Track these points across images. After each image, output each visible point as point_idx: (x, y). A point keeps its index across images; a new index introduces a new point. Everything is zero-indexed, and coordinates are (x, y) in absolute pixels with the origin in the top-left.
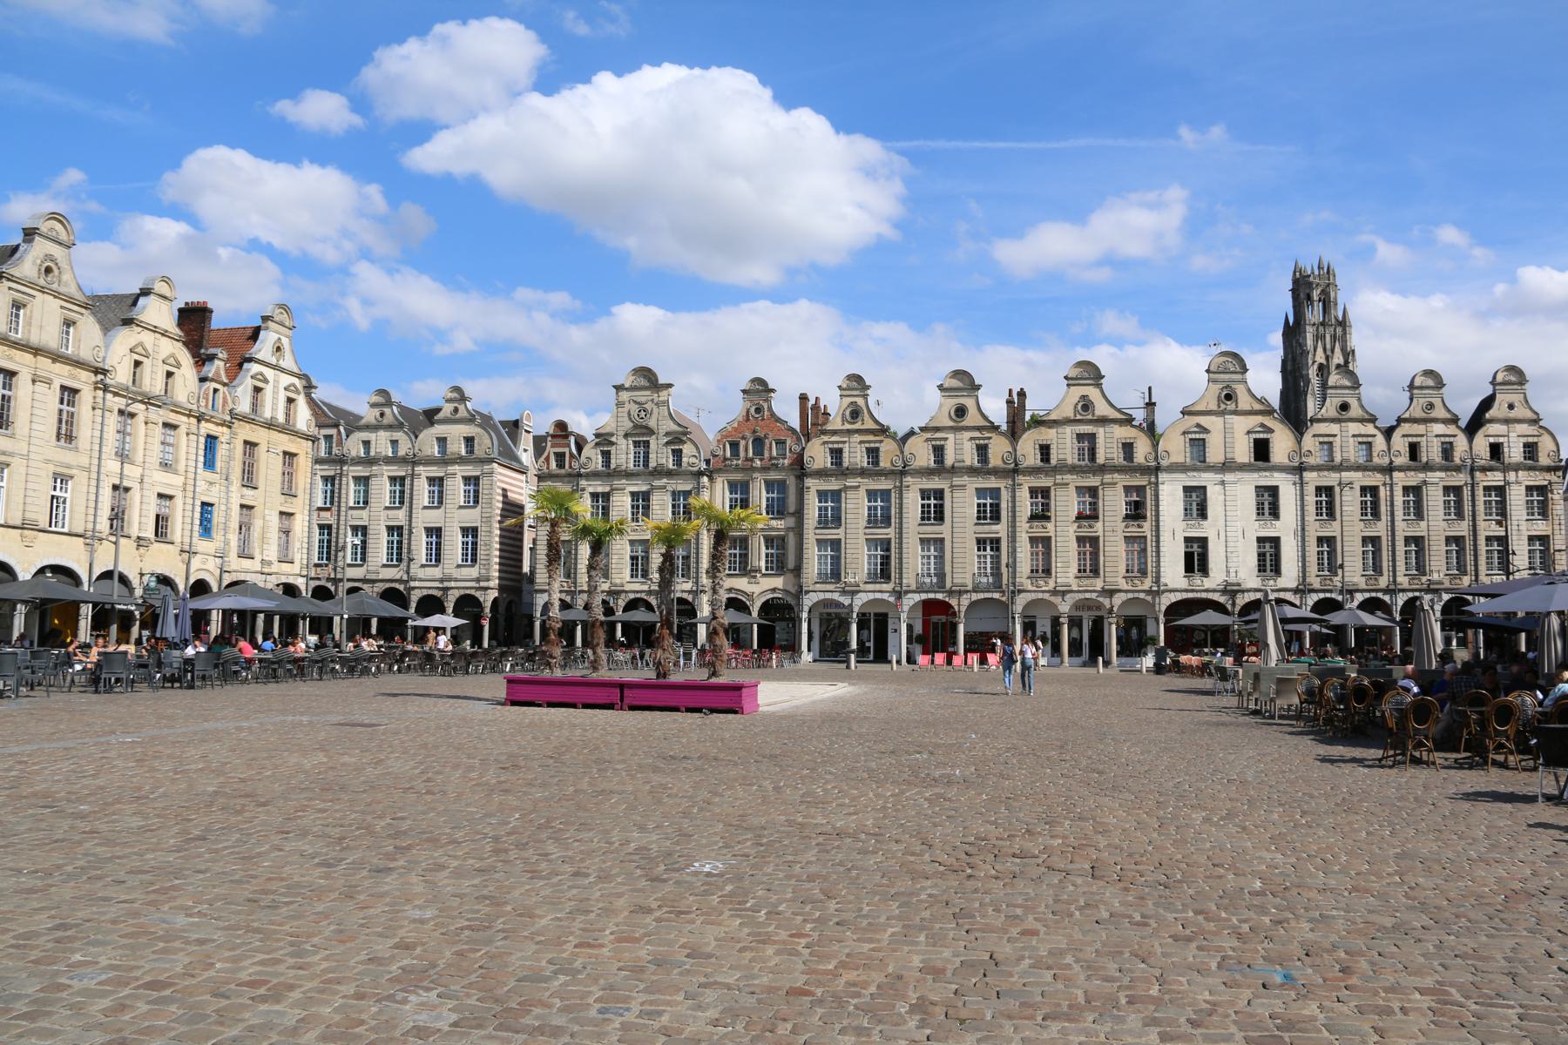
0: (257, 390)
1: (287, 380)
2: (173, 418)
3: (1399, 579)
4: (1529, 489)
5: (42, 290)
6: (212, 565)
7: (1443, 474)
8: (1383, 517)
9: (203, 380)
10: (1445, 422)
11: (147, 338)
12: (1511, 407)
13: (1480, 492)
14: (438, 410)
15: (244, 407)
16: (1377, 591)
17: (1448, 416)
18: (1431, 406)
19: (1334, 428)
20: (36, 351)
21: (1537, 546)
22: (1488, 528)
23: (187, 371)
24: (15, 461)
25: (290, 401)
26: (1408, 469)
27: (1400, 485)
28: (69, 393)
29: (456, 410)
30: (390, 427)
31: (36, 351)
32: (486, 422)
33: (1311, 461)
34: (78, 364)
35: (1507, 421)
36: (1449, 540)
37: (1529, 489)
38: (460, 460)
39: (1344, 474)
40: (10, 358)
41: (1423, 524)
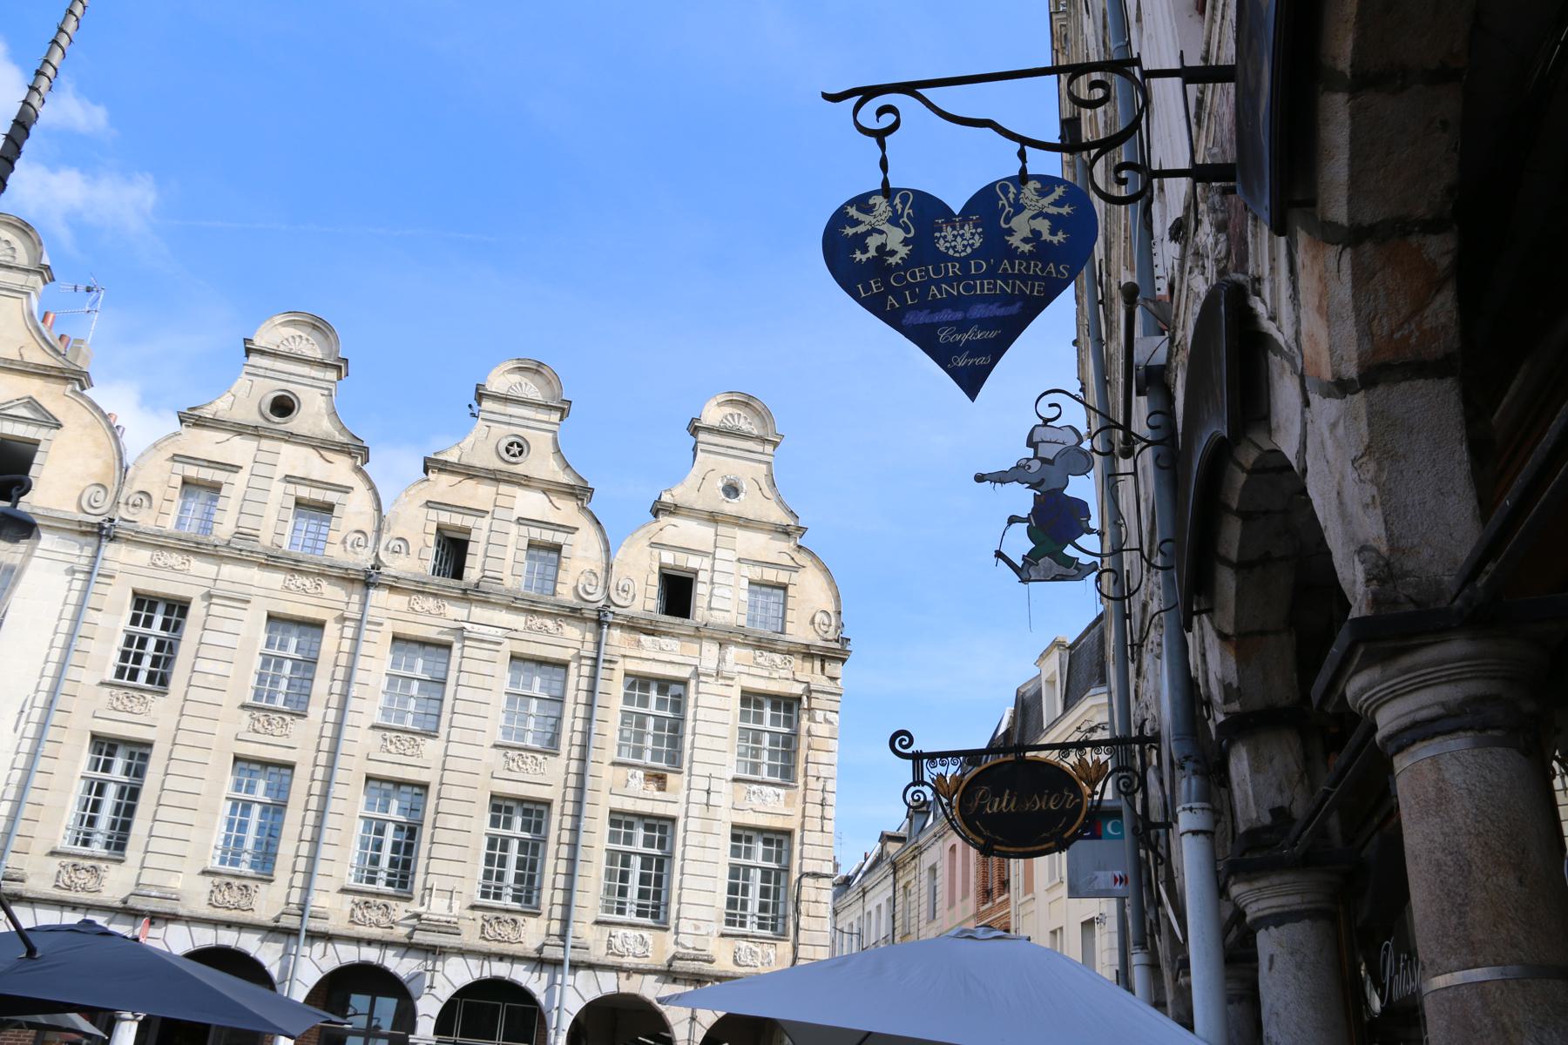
3: (318, 901)
4: (750, 699)
7: (517, 621)
8: (315, 711)
10: (550, 488)
12: (732, 490)
13: (614, 690)
16: (241, 926)
17: (565, 478)
18: (518, 448)
19: (239, 449)
21: (758, 855)
22: (619, 787)
26: (418, 589)
27: (389, 629)
33: (145, 520)
35: (713, 518)
36: (501, 806)
37: (750, 699)
39: (228, 570)
41: (431, 749)
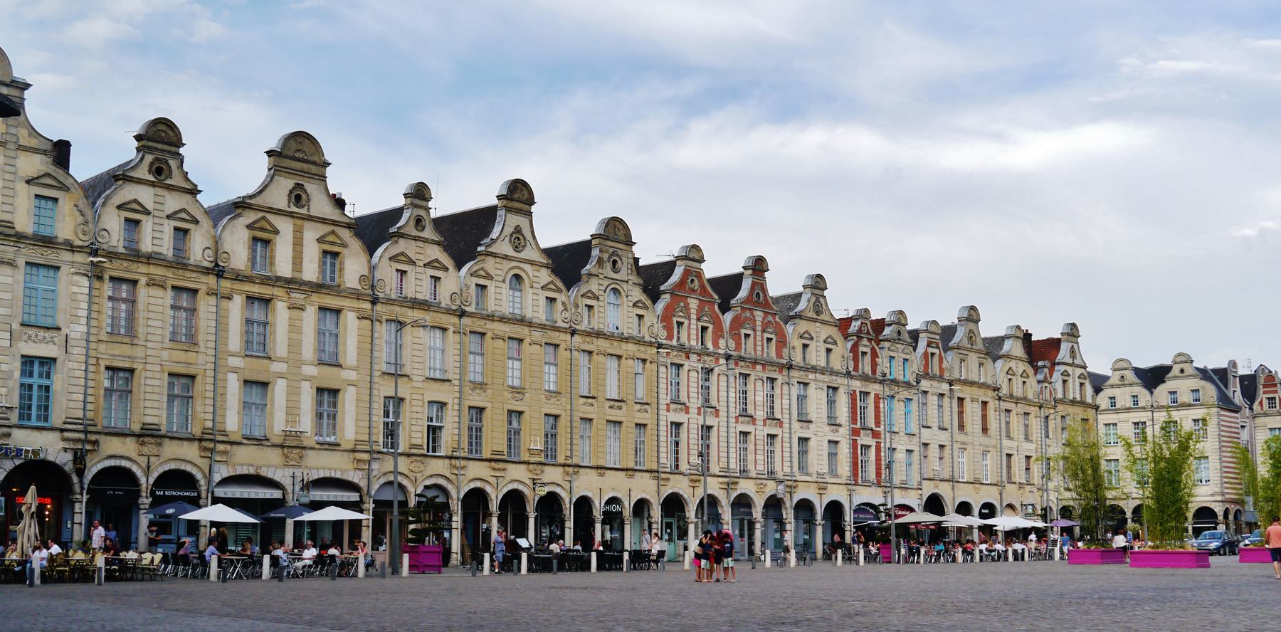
0: (1065, 381)
1: (1079, 371)
2: (1027, 409)
5: (971, 350)
6: (1053, 496)
9: (1039, 382)
11: (1013, 364)
14: (1167, 369)
15: (1060, 395)
20: (972, 384)
23: (1032, 381)
24: (968, 447)
25: (1082, 384)
28: (985, 403)
29: (1182, 371)
30: (1131, 385)
31: (972, 384)
32: (1204, 374)
38: (1190, 405)
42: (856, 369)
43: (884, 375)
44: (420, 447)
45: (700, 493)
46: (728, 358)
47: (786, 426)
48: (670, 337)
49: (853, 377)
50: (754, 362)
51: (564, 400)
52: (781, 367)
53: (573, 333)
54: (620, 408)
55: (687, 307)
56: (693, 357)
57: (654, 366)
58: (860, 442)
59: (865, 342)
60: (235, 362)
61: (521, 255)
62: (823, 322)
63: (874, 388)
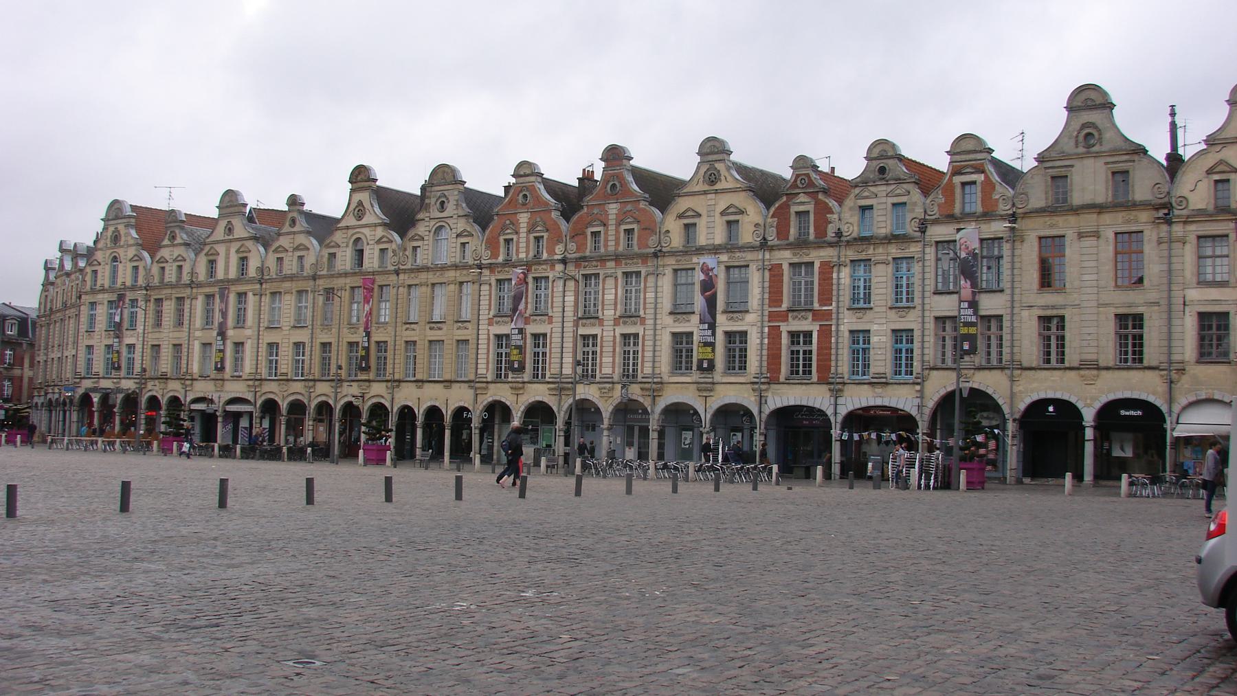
5: (1080, 157)
34: (1134, 206)
40: (1051, 226)
42: (782, 232)
43: (839, 234)
44: (286, 374)
45: (568, 402)
46: (564, 261)
47: (650, 322)
48: (495, 255)
49: (771, 249)
50: (602, 260)
51: (390, 329)
52: (644, 258)
53: (397, 273)
54: (440, 329)
55: (515, 224)
56: (611, 264)
57: (476, 286)
58: (784, 328)
59: (802, 198)
60: (198, 334)
61: (363, 222)
62: (716, 192)
63: (818, 257)
